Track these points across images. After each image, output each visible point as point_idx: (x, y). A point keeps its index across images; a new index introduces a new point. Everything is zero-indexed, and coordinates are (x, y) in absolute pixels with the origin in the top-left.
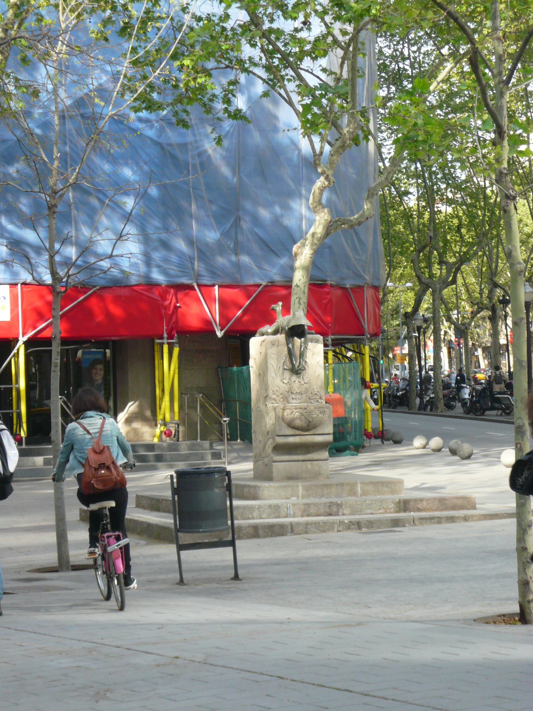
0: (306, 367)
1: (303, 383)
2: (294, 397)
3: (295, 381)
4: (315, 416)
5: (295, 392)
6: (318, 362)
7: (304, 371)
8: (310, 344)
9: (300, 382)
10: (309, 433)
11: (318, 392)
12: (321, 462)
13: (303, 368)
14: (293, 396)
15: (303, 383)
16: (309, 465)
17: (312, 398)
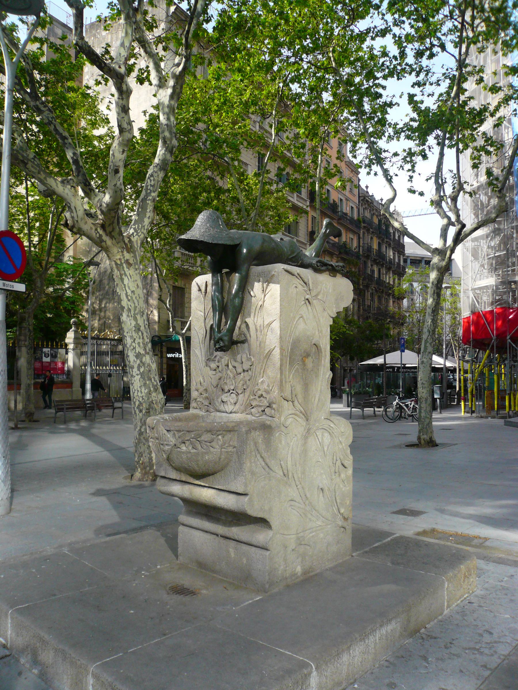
0: (248, 335)
1: (240, 370)
2: (225, 399)
3: (227, 365)
4: (167, 448)
5: (226, 389)
6: (269, 324)
7: (246, 345)
8: (256, 284)
9: (235, 367)
10: (203, 484)
11: (267, 392)
12: (254, 549)
13: (242, 338)
14: (224, 397)
15: (240, 370)
16: (232, 548)
17: (254, 403)
